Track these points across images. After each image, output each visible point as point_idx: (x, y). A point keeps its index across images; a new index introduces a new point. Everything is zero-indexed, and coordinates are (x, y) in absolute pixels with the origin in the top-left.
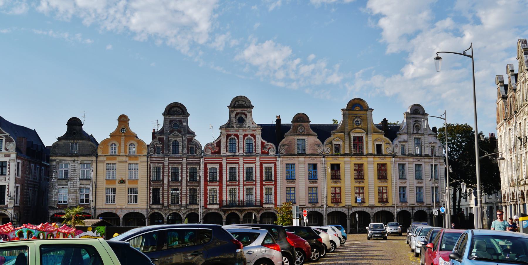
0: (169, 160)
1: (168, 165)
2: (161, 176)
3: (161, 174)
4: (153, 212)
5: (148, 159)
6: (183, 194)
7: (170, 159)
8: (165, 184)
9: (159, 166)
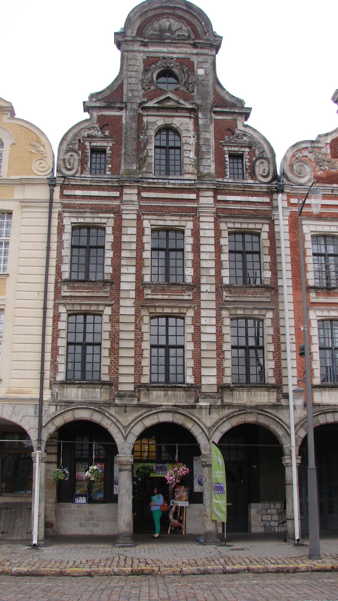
0: (141, 198)
1: (139, 216)
2: (108, 262)
3: (109, 254)
4: (69, 417)
5: (52, 192)
6: (204, 338)
7: (144, 194)
8: (122, 295)
9: (97, 220)
